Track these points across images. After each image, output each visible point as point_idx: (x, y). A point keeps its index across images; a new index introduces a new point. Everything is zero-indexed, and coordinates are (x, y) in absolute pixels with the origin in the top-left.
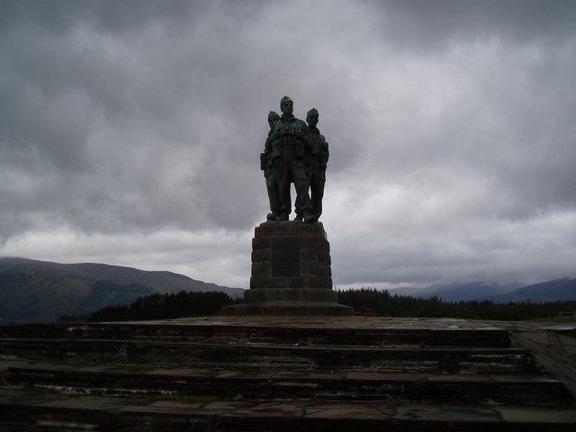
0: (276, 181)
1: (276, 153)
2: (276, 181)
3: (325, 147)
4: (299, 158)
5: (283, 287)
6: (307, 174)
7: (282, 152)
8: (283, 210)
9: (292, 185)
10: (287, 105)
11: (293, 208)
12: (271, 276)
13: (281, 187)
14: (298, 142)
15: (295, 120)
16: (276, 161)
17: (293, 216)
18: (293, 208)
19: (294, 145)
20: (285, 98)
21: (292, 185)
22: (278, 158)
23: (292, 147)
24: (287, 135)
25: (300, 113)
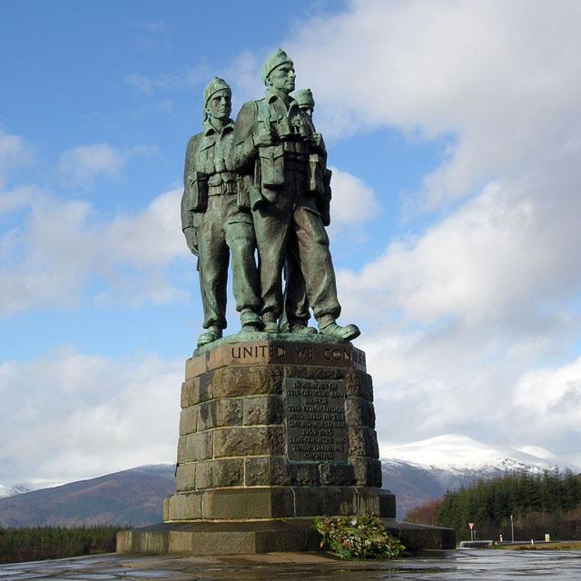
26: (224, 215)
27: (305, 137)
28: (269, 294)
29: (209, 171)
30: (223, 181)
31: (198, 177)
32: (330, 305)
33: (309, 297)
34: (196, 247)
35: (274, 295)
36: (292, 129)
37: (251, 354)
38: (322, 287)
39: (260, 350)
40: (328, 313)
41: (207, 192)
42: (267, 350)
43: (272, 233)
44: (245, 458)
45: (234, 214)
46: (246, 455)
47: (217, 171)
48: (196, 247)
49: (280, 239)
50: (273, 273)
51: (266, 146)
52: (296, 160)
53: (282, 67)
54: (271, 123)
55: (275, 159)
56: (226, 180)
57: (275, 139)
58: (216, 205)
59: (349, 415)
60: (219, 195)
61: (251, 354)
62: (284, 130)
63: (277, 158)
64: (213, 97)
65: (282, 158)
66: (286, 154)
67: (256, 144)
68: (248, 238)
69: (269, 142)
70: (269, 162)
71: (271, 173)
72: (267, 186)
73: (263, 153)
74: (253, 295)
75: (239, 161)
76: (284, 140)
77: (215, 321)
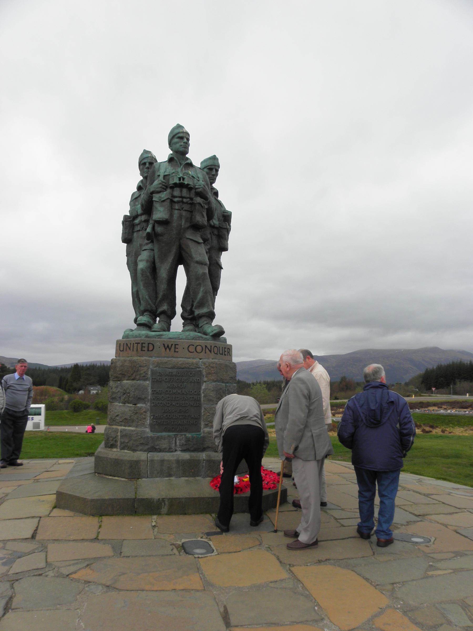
0: (154, 263)
1: (160, 213)
2: (154, 263)
3: (227, 217)
4: (196, 227)
5: (170, 450)
6: (207, 253)
7: (171, 215)
8: (163, 312)
9: (181, 269)
10: (179, 139)
11: (179, 309)
12: (148, 430)
13: (163, 273)
14: (198, 200)
15: (190, 165)
16: (159, 229)
17: (177, 324)
18: (179, 309)
19: (192, 204)
20: (179, 126)
21: (181, 269)
22: (164, 223)
23: (186, 207)
24: (181, 186)
25: (197, 156)
26: (141, 245)
29: (134, 214)
32: (205, 310)
36: (180, 179)
37: (130, 349)
38: (200, 295)
39: (135, 345)
41: (133, 229)
42: (139, 346)
44: (120, 428)
45: (147, 244)
46: (121, 425)
50: (163, 286)
52: (182, 202)
54: (165, 176)
58: (139, 238)
59: (204, 396)
61: (130, 349)
65: (169, 201)
67: (152, 190)
68: (147, 261)
73: (156, 197)
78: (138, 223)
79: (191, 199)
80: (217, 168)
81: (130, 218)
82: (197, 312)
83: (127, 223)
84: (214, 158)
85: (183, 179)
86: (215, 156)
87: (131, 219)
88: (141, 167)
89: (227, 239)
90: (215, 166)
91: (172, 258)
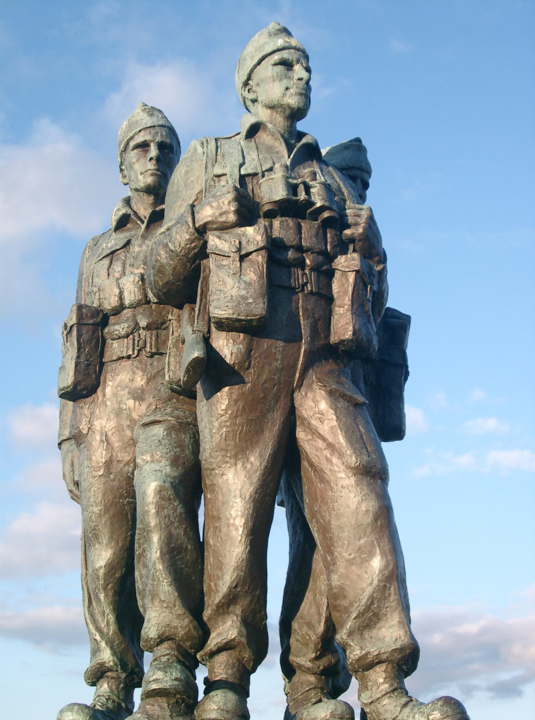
27: (322, 209)
28: (231, 599)
30: (136, 327)
31: (80, 317)
33: (335, 615)
34: (77, 484)
35: (238, 609)
40: (380, 662)
43: (241, 444)
47: (127, 302)
48: (77, 484)
49: (257, 460)
51: (224, 228)
53: (276, 57)
55: (242, 258)
56: (143, 323)
57: (248, 210)
58: (122, 382)
60: (129, 357)
62: (272, 190)
63: (248, 254)
64: (132, 144)
66: (274, 248)
69: (232, 218)
70: (233, 263)
71: (232, 288)
72: (224, 325)
74: (179, 609)
75: (162, 266)
76: (270, 215)
77: (110, 670)
78: (123, 333)
79: (330, 258)
80: (365, 175)
81: (92, 317)
82: (355, 653)
83: (85, 330)
84: (357, 146)
85: (307, 189)
86: (358, 140)
87: (99, 320)
88: (132, 155)
89: (400, 399)
90: (361, 169)
91: (269, 451)
